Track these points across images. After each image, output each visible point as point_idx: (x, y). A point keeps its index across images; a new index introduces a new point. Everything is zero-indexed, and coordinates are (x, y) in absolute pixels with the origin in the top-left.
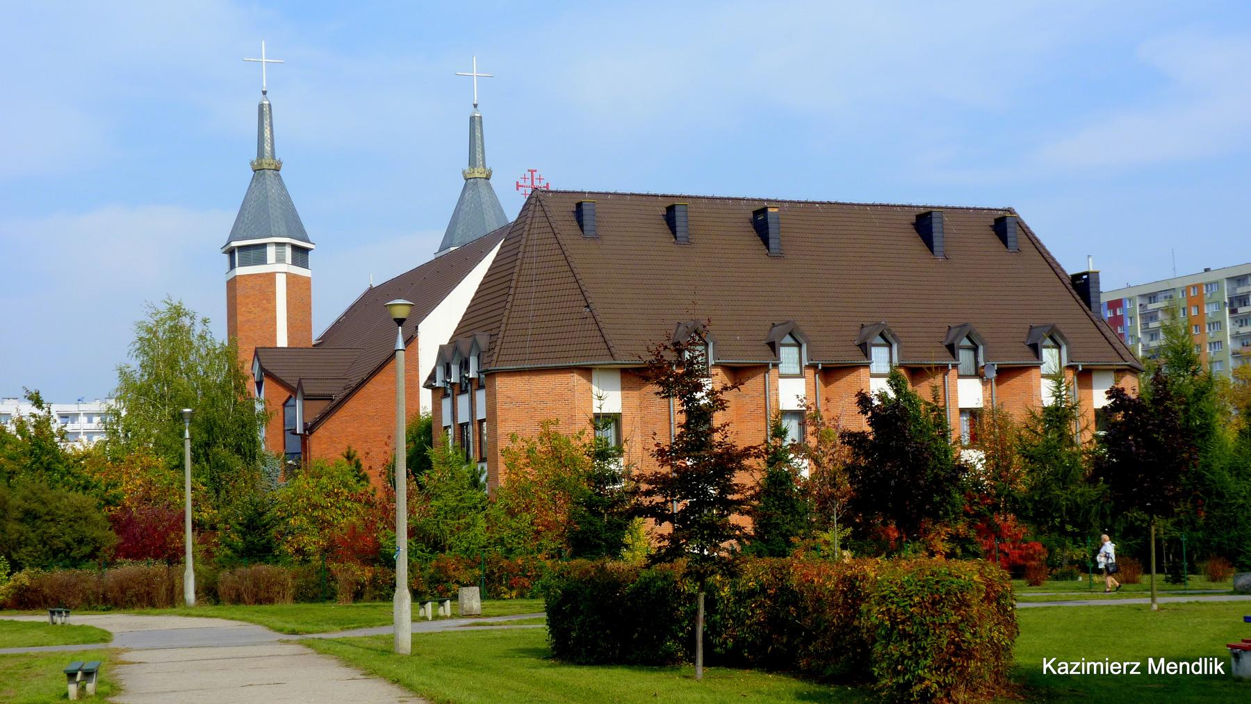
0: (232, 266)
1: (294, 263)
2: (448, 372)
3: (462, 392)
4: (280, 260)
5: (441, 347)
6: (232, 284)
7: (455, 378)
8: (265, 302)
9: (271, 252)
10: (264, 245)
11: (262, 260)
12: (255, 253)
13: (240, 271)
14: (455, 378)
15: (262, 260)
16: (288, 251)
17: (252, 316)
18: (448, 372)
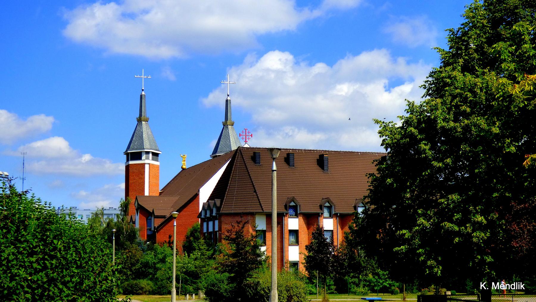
0: (128, 160)
1: (153, 159)
2: (206, 214)
3: (211, 220)
4: (147, 158)
5: (204, 203)
6: (128, 167)
7: (208, 215)
8: (140, 175)
9: (144, 157)
10: (141, 152)
11: (140, 159)
12: (137, 156)
13: (131, 162)
14: (208, 215)
15: (140, 159)
16: (151, 155)
17: (135, 181)
18: (206, 214)
